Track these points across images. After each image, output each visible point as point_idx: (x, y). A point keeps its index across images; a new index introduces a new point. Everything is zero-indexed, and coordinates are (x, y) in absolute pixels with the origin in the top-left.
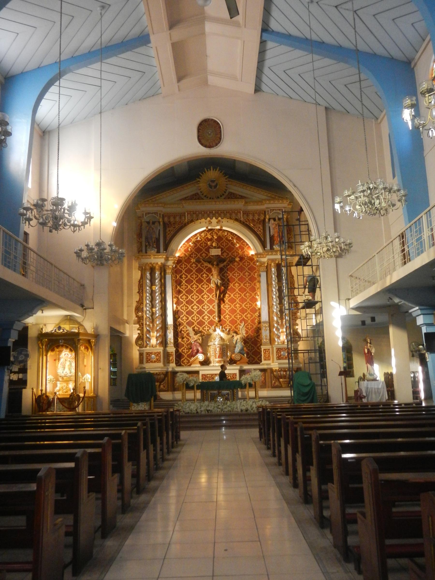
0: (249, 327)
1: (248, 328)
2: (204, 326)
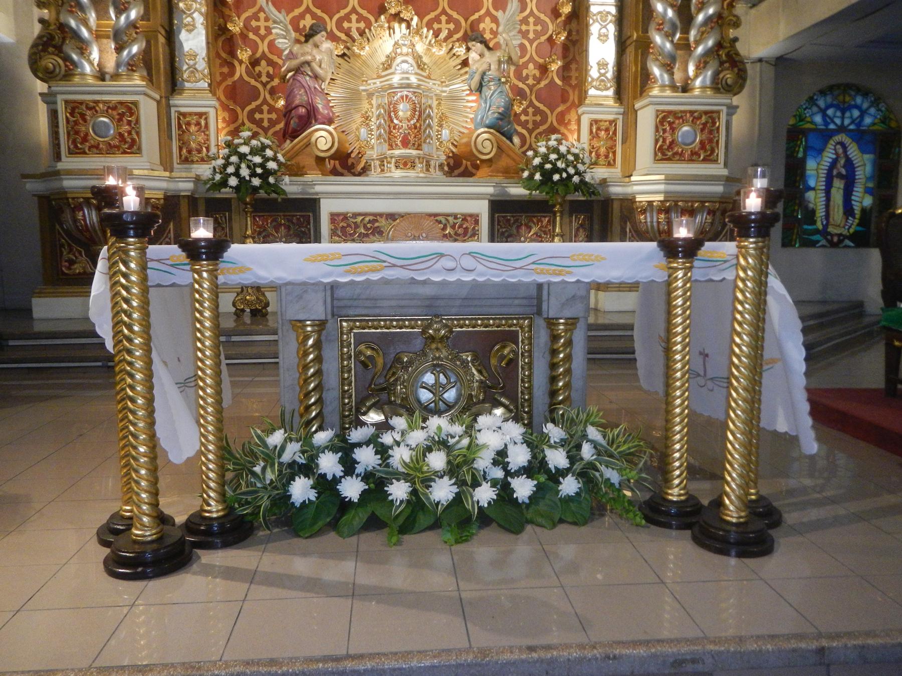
0: (531, 28)
1: (525, 34)
2: (342, 13)
